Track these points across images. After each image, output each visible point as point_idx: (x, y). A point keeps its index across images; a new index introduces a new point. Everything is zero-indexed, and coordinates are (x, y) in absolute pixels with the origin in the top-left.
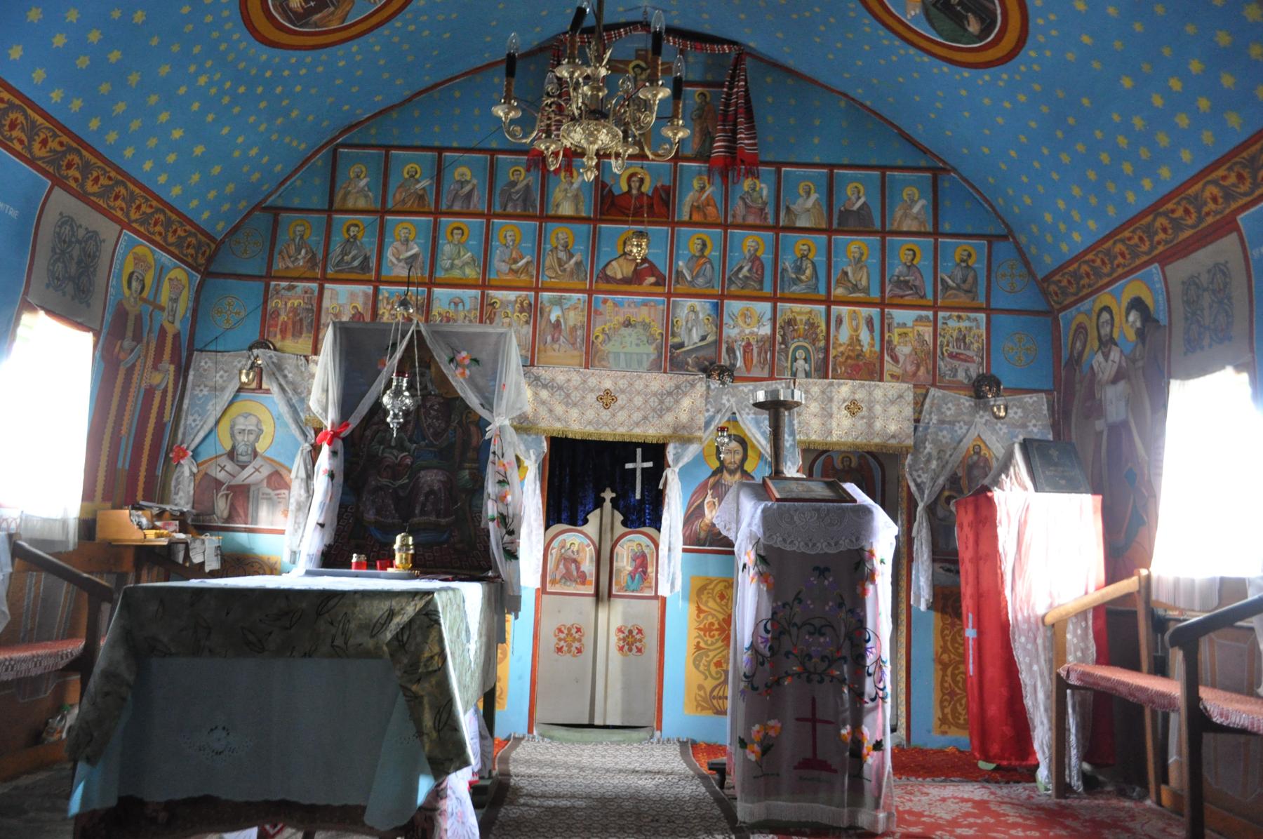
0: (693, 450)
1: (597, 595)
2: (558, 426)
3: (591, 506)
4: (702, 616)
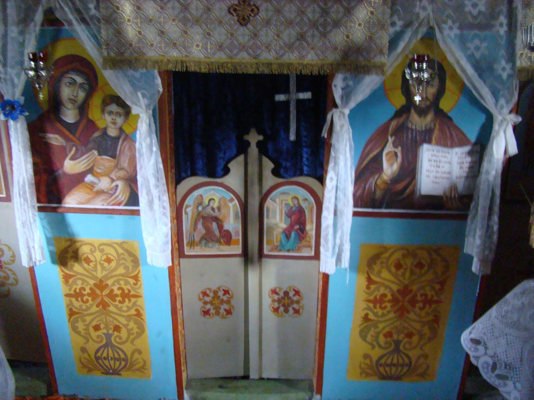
0: (369, 83)
1: (246, 255)
2: (175, 54)
3: (234, 151)
4: (373, 287)
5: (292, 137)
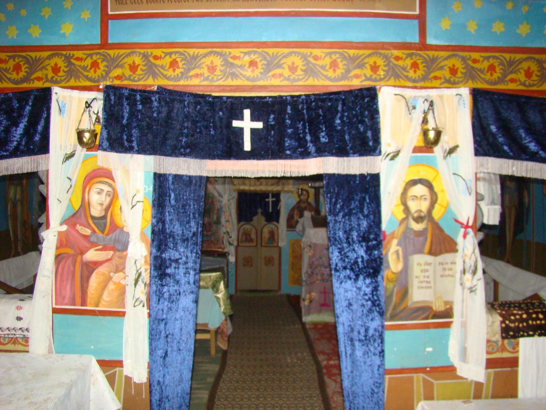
5: (270, 210)
